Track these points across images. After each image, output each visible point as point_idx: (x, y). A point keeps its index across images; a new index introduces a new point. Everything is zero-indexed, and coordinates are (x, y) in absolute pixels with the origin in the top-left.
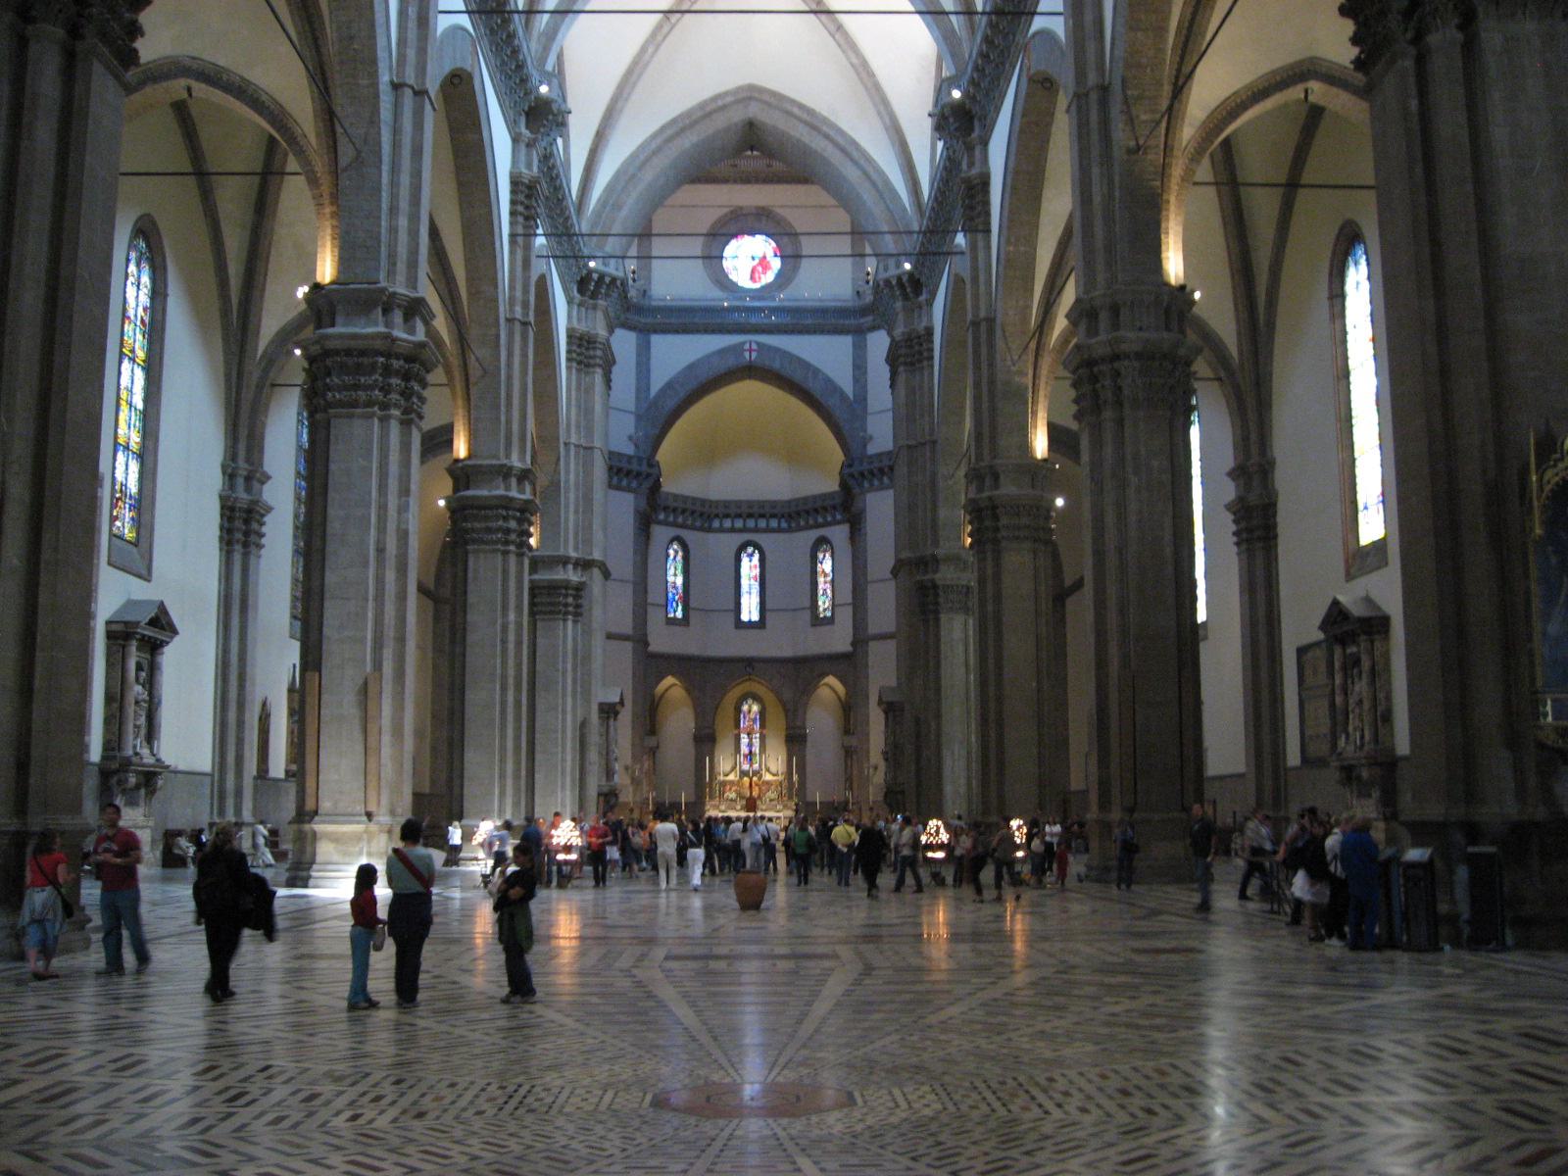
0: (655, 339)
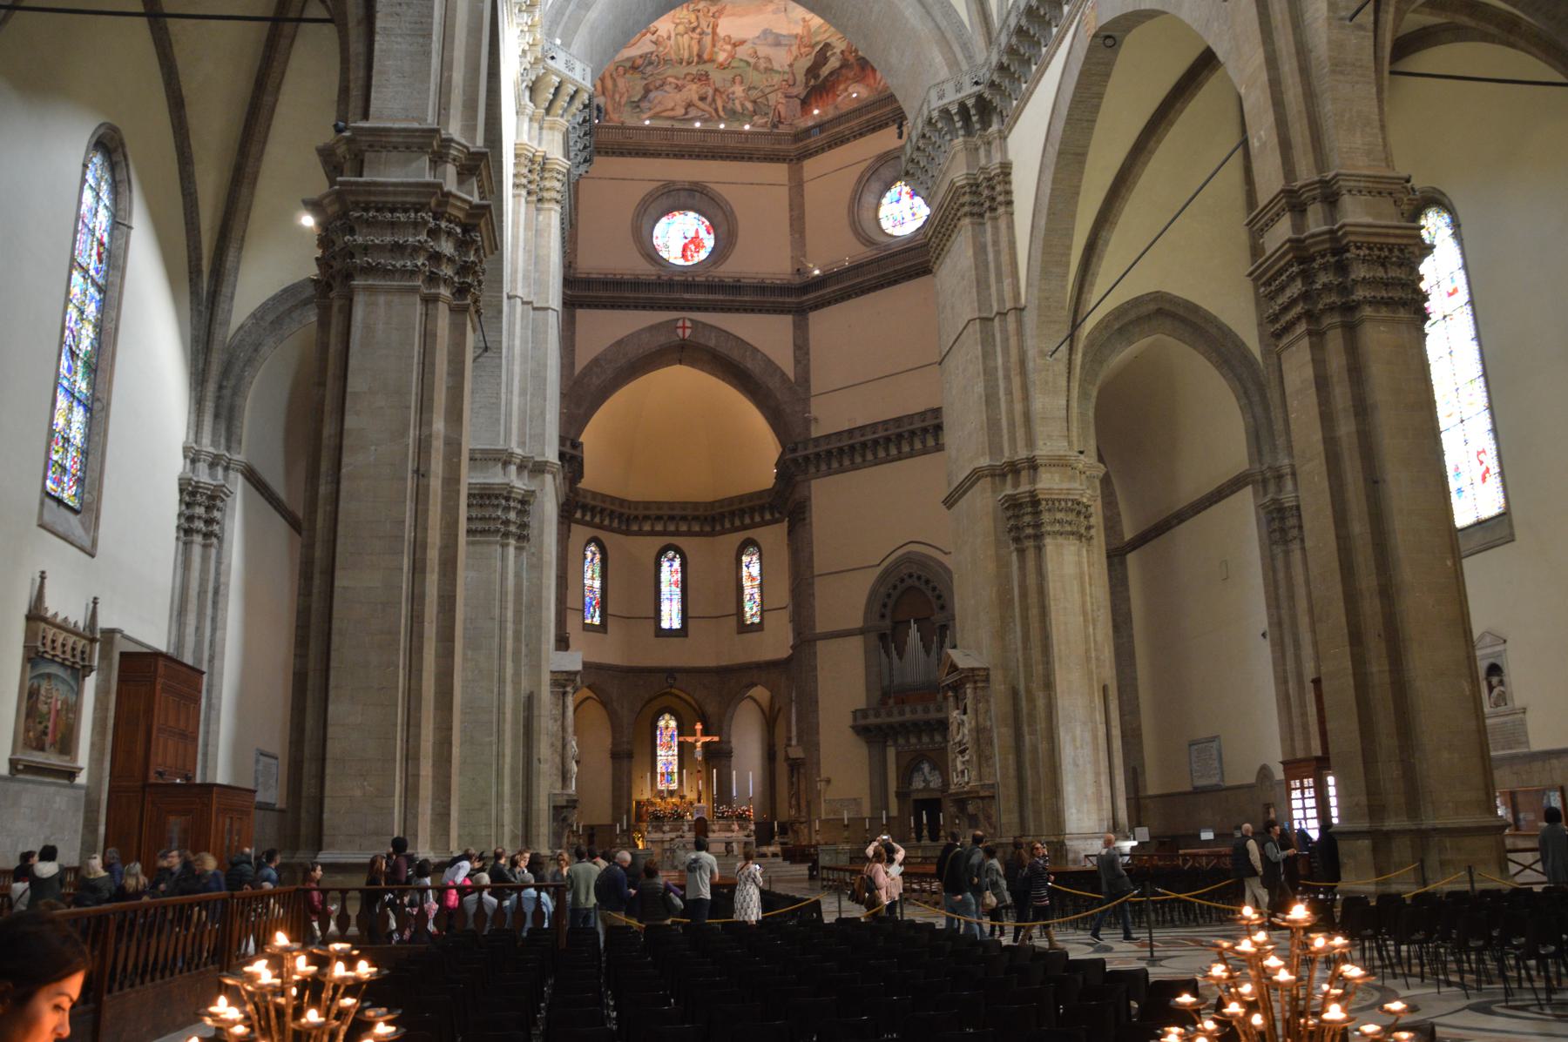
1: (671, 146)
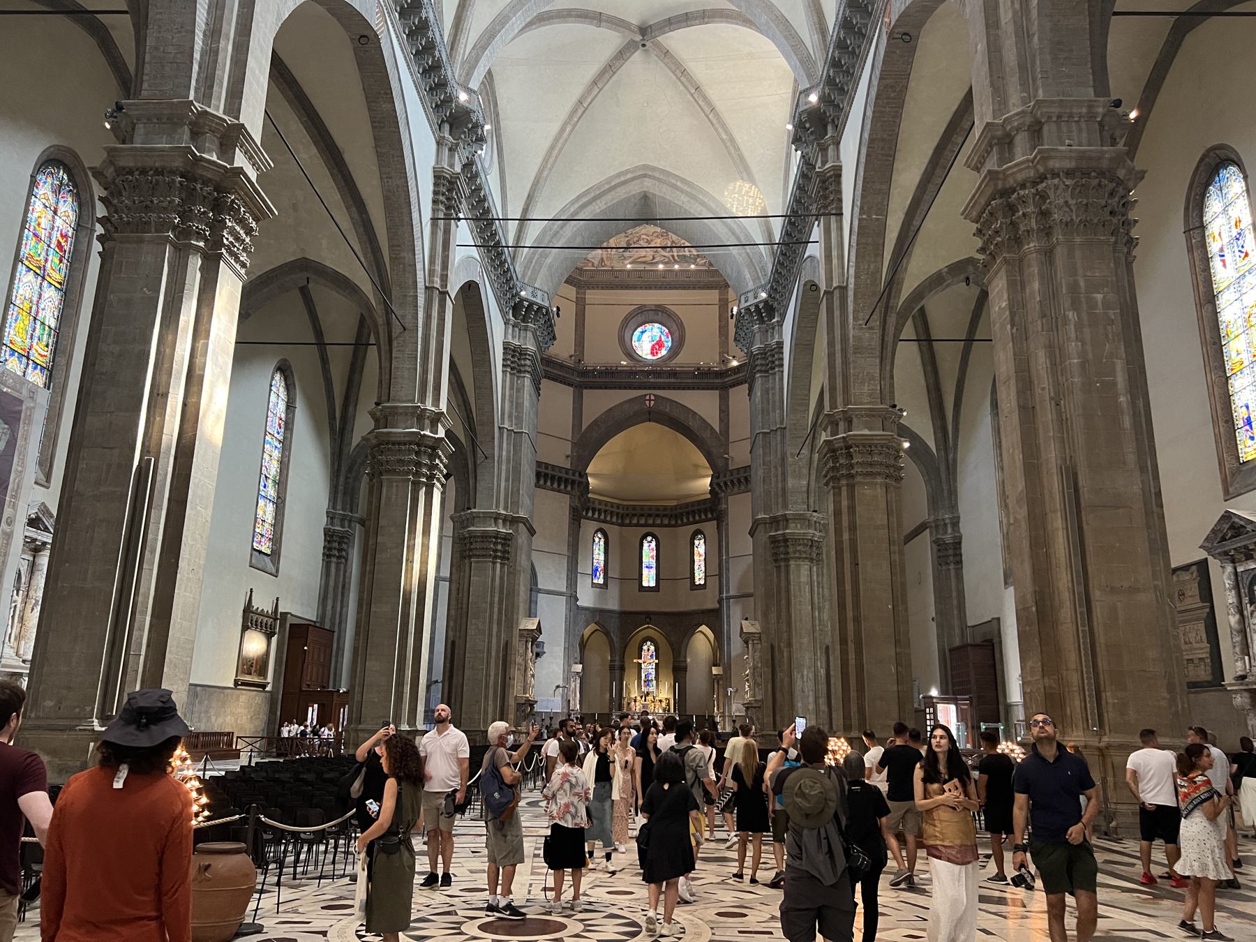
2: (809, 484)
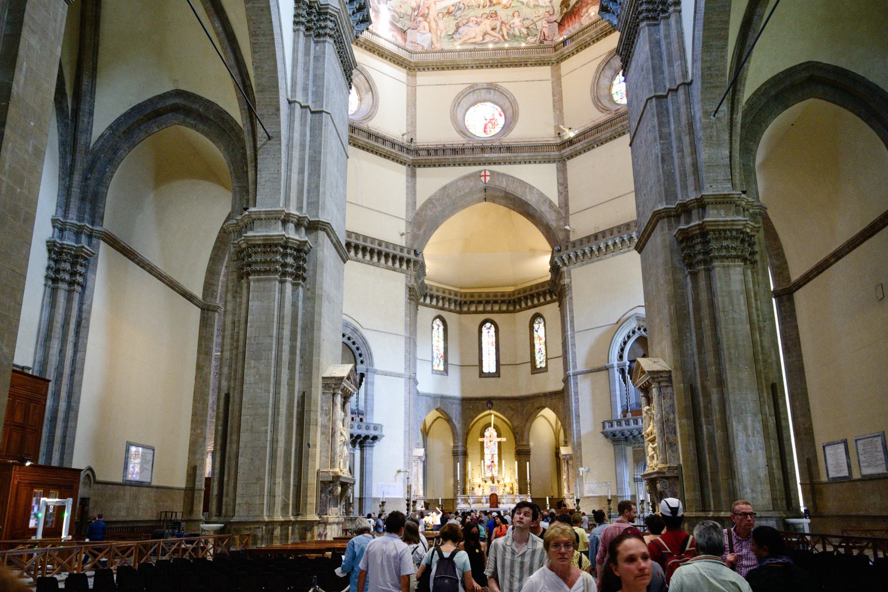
0: (419, 171)
1: (474, 60)
2: (731, 156)
